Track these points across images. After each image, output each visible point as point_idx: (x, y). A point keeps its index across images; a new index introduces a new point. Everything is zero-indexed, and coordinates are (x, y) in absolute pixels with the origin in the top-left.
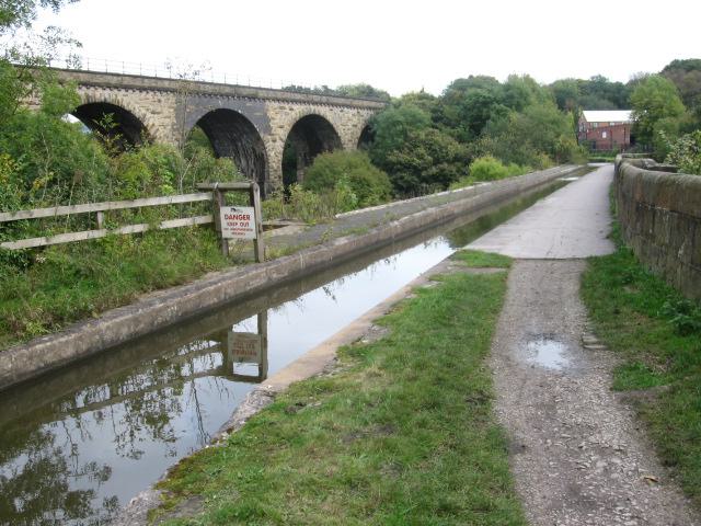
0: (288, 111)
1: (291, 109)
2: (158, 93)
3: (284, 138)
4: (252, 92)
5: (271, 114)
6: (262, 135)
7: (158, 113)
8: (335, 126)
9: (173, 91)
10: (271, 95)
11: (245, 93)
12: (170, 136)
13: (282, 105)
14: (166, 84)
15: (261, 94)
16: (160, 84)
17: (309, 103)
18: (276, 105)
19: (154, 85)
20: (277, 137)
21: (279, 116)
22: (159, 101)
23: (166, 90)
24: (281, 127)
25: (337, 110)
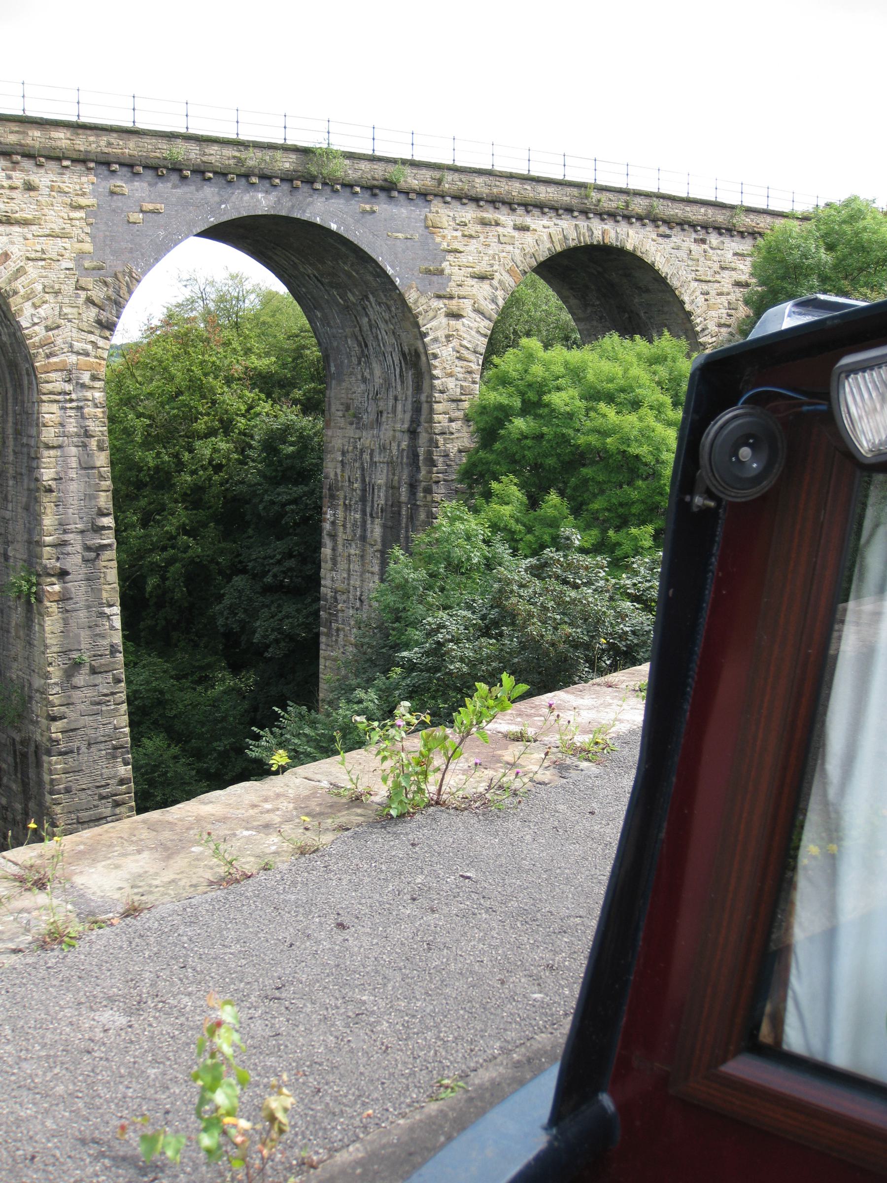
0: (509, 230)
1: (524, 229)
2: (27, 164)
3: (490, 308)
4: (379, 171)
5: (449, 237)
6: (411, 297)
7: (25, 223)
8: (675, 283)
9: (81, 160)
10: (451, 182)
11: (352, 175)
12: (68, 288)
13: (490, 214)
14: (61, 139)
15: (413, 180)
16: (35, 138)
17: (585, 212)
18: (469, 213)
19: (12, 139)
20: (467, 304)
21: (474, 245)
22: (30, 187)
23: (56, 157)
24: (482, 278)
25: (685, 241)
